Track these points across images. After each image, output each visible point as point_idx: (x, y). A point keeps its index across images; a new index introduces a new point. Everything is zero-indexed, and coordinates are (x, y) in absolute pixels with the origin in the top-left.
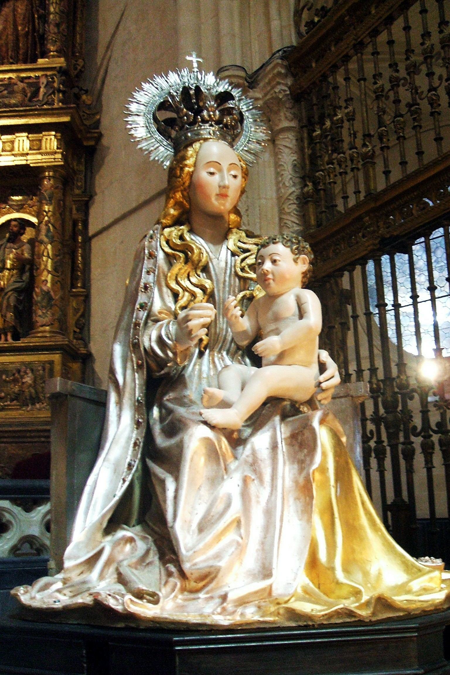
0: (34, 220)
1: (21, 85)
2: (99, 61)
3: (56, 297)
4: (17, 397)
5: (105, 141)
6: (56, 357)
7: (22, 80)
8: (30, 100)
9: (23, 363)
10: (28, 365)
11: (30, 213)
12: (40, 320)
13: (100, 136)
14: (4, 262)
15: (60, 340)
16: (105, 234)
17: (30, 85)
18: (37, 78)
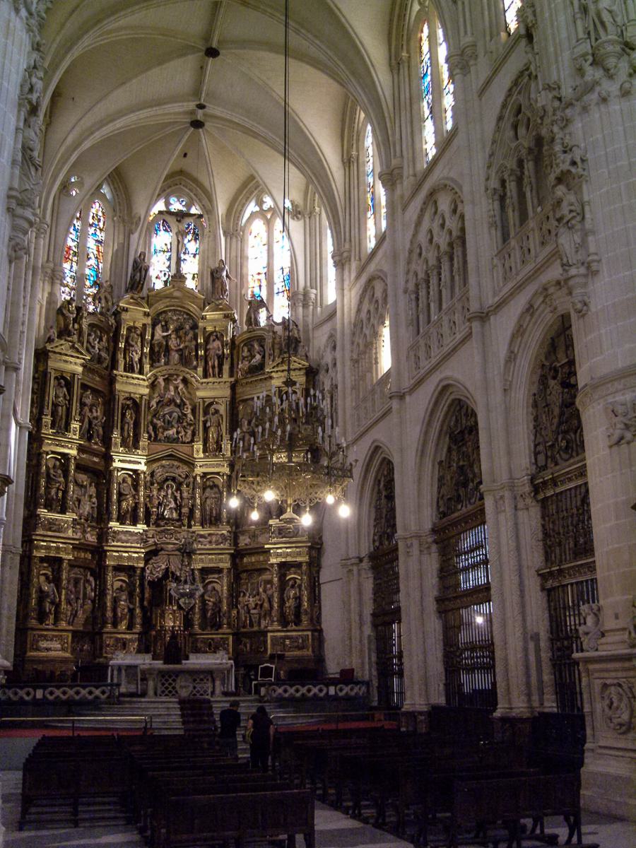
3: (309, 611)
4: (296, 647)
6: (309, 633)
12: (304, 620)
15: (310, 627)
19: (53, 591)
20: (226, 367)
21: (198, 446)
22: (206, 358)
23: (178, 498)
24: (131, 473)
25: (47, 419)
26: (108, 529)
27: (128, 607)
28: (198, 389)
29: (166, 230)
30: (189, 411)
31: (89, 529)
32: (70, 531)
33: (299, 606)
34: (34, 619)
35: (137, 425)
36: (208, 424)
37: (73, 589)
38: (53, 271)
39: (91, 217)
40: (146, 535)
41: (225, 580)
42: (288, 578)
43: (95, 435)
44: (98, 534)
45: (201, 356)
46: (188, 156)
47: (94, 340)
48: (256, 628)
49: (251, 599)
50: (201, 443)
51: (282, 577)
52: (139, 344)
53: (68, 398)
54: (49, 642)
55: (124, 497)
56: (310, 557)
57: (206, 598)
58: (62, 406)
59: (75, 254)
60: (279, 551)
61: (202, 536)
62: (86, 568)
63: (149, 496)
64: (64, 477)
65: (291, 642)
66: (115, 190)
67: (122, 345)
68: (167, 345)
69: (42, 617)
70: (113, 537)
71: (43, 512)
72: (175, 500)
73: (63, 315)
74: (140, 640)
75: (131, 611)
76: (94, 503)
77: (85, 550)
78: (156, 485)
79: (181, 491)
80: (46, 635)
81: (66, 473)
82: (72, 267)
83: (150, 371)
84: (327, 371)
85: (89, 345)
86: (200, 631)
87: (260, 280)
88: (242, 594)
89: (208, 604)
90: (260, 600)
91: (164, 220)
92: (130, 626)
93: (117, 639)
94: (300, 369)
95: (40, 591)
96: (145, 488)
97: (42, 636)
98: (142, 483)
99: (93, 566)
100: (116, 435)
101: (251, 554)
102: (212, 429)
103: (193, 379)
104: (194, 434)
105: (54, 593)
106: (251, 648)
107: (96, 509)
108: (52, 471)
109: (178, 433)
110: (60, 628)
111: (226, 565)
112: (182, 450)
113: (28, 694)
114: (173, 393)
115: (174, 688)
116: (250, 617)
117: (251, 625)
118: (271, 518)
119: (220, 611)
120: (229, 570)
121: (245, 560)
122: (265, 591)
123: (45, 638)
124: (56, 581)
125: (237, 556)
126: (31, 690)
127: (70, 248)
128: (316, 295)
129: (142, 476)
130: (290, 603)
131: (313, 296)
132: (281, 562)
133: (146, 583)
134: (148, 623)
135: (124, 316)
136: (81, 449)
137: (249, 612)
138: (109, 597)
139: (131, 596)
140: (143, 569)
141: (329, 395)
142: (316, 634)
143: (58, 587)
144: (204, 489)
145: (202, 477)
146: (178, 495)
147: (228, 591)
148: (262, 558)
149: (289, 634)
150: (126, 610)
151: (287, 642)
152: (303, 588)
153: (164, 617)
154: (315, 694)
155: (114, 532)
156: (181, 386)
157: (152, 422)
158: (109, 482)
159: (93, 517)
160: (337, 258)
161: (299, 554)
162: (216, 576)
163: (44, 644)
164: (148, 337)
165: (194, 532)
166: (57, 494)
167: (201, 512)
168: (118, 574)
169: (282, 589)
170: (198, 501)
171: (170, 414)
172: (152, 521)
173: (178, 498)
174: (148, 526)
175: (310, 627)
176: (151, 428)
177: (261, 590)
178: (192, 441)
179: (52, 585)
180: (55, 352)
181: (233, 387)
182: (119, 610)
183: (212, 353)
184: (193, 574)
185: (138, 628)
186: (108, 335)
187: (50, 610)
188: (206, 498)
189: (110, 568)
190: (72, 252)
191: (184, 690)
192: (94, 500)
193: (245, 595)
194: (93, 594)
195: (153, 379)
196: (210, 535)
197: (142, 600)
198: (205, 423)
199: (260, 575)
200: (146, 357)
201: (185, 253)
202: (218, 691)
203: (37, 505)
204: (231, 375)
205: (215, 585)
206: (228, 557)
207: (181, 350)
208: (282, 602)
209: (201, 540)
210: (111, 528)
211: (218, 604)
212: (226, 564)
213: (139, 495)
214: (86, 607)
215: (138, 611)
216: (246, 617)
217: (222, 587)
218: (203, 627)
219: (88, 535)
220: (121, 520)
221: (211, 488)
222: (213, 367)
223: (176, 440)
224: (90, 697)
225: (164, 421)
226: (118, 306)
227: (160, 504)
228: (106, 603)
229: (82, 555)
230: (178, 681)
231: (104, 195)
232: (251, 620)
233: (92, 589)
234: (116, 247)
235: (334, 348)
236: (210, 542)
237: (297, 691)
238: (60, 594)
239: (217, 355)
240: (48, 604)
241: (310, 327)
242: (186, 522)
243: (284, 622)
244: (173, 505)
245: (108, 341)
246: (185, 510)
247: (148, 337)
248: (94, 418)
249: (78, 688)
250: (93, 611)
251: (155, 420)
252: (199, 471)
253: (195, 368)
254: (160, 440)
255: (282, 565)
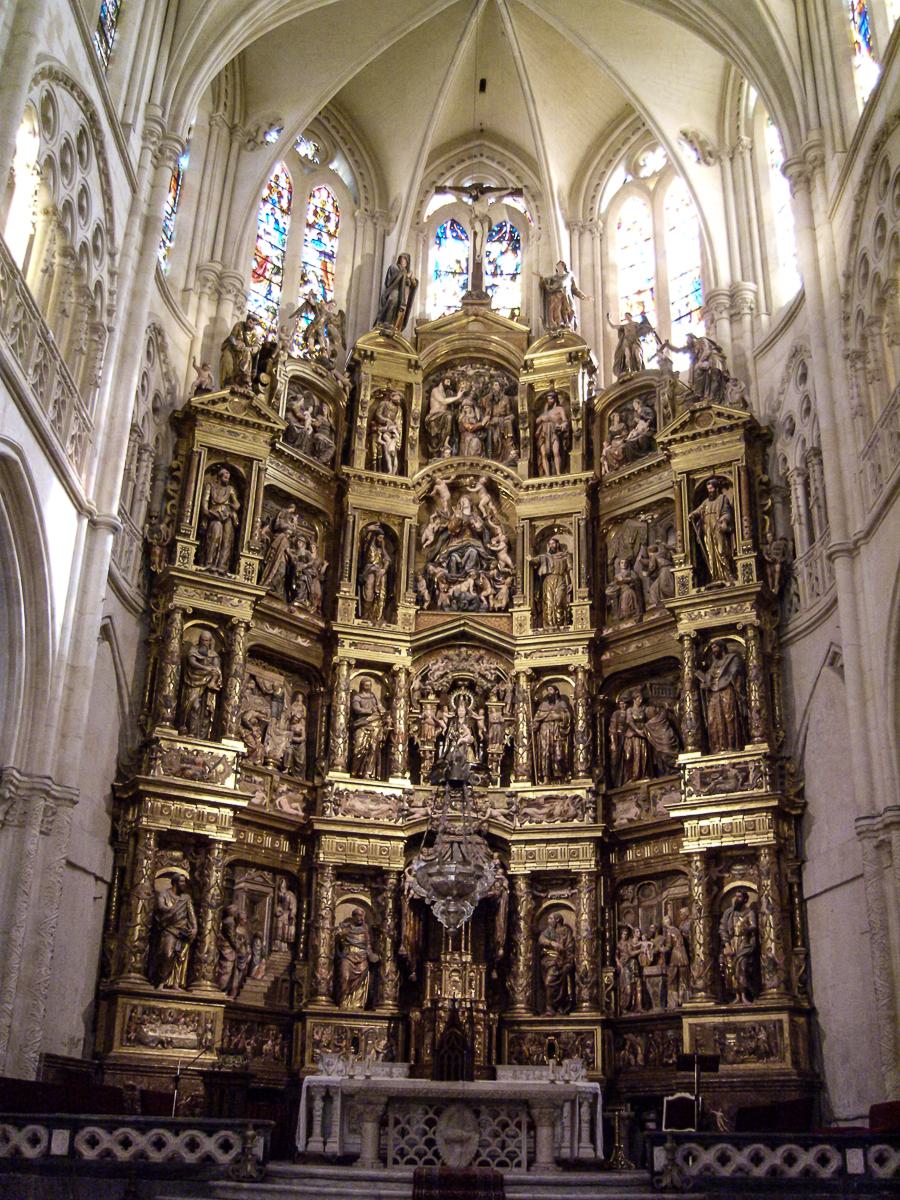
0: (755, 887)
1: (734, 772)
2: (798, 728)
4: (754, 1051)
5: (810, 809)
6: (784, 1017)
7: (734, 766)
8: (742, 785)
9: (756, 1022)
10: (761, 1024)
11: (751, 881)
12: (768, 983)
13: (806, 804)
14: (733, 929)
15: (786, 1002)
16: (817, 899)
17: (741, 770)
18: (746, 763)
19: (187, 909)
20: (576, 453)
21: (523, 613)
22: (535, 440)
23: (481, 723)
24: (380, 674)
25: (188, 547)
26: (325, 785)
27: (368, 959)
28: (519, 501)
29: (457, 238)
30: (503, 545)
31: (284, 787)
32: (230, 783)
33: (756, 953)
34: (138, 971)
35: (392, 577)
36: (543, 570)
37: (243, 915)
38: (220, 277)
39: (311, 212)
40: (410, 802)
41: (585, 898)
42: (727, 889)
43: (301, 593)
44: (305, 799)
45: (525, 438)
46: (488, 87)
47: (303, 409)
48: (656, 1010)
49: (645, 944)
50: (527, 607)
51: (713, 886)
52: (399, 422)
53: (237, 505)
54: (169, 1027)
55: (360, 721)
56: (777, 835)
57: (543, 940)
58: (224, 522)
59: (278, 271)
60: (704, 823)
61: (532, 803)
62: (274, 871)
63: (418, 721)
64: (222, 668)
65: (738, 1039)
66: (357, 166)
67: (363, 423)
68: (455, 421)
69: (156, 968)
70: (335, 802)
71: (165, 732)
72: (475, 730)
73: (233, 349)
74: (392, 1035)
75: (375, 968)
76: (299, 735)
77: (277, 832)
78: (432, 697)
79: (486, 709)
80: (161, 1011)
81: (226, 657)
82: (270, 292)
83: (421, 466)
84: (791, 432)
85: (290, 415)
86: (528, 1016)
87: (642, 303)
88: (624, 933)
89: (546, 955)
90: (664, 944)
91: (454, 222)
92: (372, 1002)
93: (339, 1030)
94: (731, 428)
95: (158, 911)
96: (410, 703)
97: (152, 1010)
98: (402, 692)
99: (294, 870)
100: (347, 589)
101: (641, 841)
102: (550, 582)
103: (509, 482)
104: (512, 593)
105: (188, 916)
106: (646, 1057)
107: (303, 747)
108: (194, 651)
109: (478, 588)
110: (196, 993)
111: (586, 865)
112: (484, 625)
113: (34, 1141)
114: (467, 512)
115: (430, 1143)
116: (643, 984)
117: (647, 1003)
118: (682, 749)
119: (573, 970)
120: (595, 876)
121: (630, 855)
122: (675, 922)
123: (162, 1017)
124: (195, 887)
125: (610, 844)
126: (42, 1131)
127: (266, 259)
128: (756, 293)
129: (402, 676)
130: (735, 946)
131: (750, 296)
132: (709, 849)
133: (406, 905)
134: (410, 993)
135: (367, 369)
136: (259, 615)
137: (640, 974)
138: (324, 935)
139: (376, 932)
140: (400, 873)
141: (799, 480)
142: (801, 1020)
143: (199, 904)
144: (536, 706)
145: (530, 679)
146: (480, 718)
147: (593, 923)
148: (666, 849)
149: (732, 1019)
150: (363, 967)
151: (731, 1038)
152: (764, 908)
153: (440, 980)
154: (807, 1171)
155: (339, 793)
156: (485, 498)
157: (426, 572)
158: (331, 692)
159: (295, 763)
160: (794, 170)
161: (752, 828)
162: (566, 892)
163: (152, 1032)
164: (416, 406)
165: (514, 795)
166: (203, 698)
167: (530, 750)
168: (347, 886)
169: (714, 917)
170: (523, 728)
171: (461, 551)
172: (424, 774)
173: (481, 723)
174: (415, 780)
175: (786, 1002)
176: (423, 583)
177: (666, 920)
178: (510, 604)
179: (185, 897)
180: (207, 413)
181: (594, 491)
182: (346, 964)
183: (546, 428)
184: (512, 886)
185: (389, 1008)
186: (336, 405)
187: (176, 954)
188: (541, 722)
189: (329, 870)
190: (269, 266)
191: (458, 1149)
192: (300, 727)
193: (630, 934)
194: (293, 929)
195: (425, 486)
196: (548, 799)
197: (396, 945)
198: (535, 566)
199: (664, 888)
200: (412, 448)
201: (494, 275)
202: (544, 1156)
203: (157, 718)
204: (589, 461)
205: (563, 913)
206: (590, 847)
207: (483, 429)
208: (715, 944)
209: (529, 811)
210: (331, 784)
211: (569, 953)
212: (584, 863)
213: (394, 718)
214: (276, 957)
215: (389, 967)
216: (633, 985)
217: (578, 914)
218: (534, 1006)
219: (283, 800)
220: (355, 767)
221: (551, 699)
222: (550, 457)
223: (473, 605)
224: (190, 1158)
225: (449, 567)
226: (354, 349)
227: (441, 738)
228: (316, 949)
229: (268, 842)
230: (442, 1124)
231: (334, 173)
232: (645, 992)
233: (290, 918)
234: (358, 261)
235: (804, 377)
236: (550, 815)
237: (757, 1159)
238: (201, 918)
239: (558, 431)
240: (171, 940)
241: (749, 354)
242: (497, 774)
243: (721, 990)
244: (467, 736)
245: (336, 415)
246: (495, 748)
247: (416, 406)
248: (301, 559)
249: (161, 1131)
250: (291, 968)
251: (431, 567)
252: (522, 664)
253: (513, 464)
254: (442, 608)
255: (712, 857)
